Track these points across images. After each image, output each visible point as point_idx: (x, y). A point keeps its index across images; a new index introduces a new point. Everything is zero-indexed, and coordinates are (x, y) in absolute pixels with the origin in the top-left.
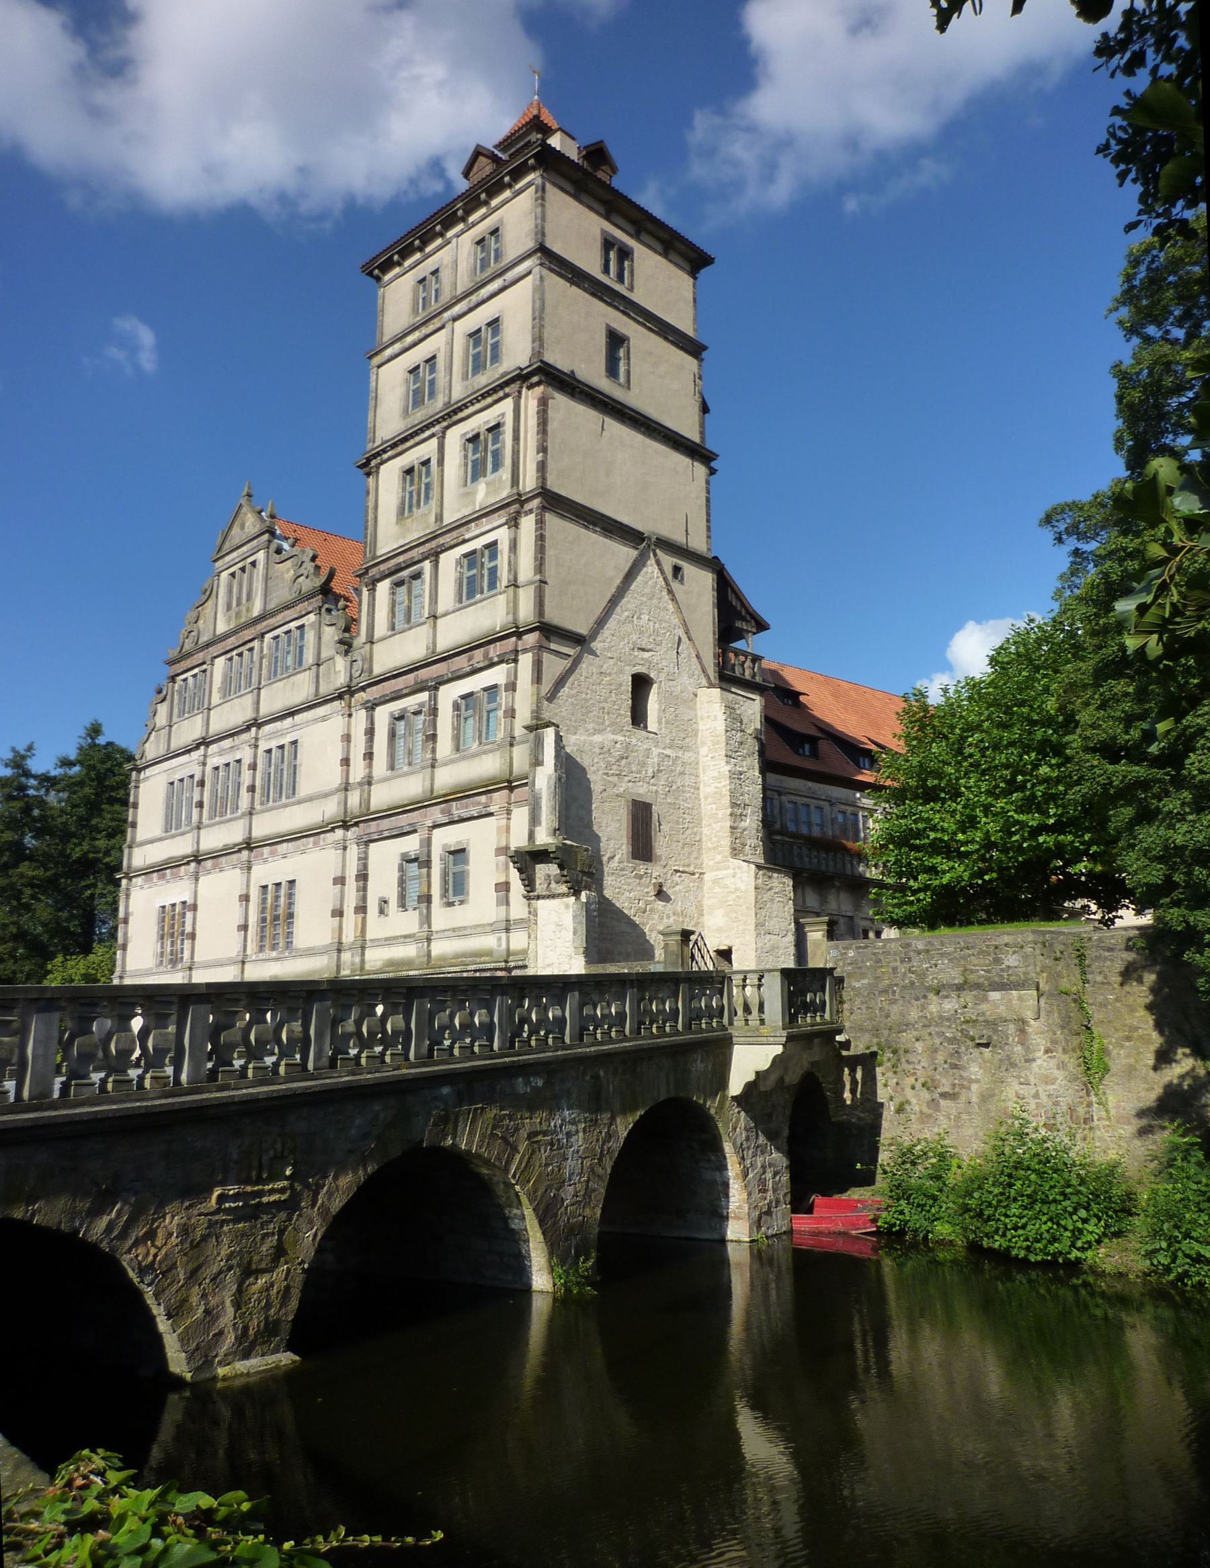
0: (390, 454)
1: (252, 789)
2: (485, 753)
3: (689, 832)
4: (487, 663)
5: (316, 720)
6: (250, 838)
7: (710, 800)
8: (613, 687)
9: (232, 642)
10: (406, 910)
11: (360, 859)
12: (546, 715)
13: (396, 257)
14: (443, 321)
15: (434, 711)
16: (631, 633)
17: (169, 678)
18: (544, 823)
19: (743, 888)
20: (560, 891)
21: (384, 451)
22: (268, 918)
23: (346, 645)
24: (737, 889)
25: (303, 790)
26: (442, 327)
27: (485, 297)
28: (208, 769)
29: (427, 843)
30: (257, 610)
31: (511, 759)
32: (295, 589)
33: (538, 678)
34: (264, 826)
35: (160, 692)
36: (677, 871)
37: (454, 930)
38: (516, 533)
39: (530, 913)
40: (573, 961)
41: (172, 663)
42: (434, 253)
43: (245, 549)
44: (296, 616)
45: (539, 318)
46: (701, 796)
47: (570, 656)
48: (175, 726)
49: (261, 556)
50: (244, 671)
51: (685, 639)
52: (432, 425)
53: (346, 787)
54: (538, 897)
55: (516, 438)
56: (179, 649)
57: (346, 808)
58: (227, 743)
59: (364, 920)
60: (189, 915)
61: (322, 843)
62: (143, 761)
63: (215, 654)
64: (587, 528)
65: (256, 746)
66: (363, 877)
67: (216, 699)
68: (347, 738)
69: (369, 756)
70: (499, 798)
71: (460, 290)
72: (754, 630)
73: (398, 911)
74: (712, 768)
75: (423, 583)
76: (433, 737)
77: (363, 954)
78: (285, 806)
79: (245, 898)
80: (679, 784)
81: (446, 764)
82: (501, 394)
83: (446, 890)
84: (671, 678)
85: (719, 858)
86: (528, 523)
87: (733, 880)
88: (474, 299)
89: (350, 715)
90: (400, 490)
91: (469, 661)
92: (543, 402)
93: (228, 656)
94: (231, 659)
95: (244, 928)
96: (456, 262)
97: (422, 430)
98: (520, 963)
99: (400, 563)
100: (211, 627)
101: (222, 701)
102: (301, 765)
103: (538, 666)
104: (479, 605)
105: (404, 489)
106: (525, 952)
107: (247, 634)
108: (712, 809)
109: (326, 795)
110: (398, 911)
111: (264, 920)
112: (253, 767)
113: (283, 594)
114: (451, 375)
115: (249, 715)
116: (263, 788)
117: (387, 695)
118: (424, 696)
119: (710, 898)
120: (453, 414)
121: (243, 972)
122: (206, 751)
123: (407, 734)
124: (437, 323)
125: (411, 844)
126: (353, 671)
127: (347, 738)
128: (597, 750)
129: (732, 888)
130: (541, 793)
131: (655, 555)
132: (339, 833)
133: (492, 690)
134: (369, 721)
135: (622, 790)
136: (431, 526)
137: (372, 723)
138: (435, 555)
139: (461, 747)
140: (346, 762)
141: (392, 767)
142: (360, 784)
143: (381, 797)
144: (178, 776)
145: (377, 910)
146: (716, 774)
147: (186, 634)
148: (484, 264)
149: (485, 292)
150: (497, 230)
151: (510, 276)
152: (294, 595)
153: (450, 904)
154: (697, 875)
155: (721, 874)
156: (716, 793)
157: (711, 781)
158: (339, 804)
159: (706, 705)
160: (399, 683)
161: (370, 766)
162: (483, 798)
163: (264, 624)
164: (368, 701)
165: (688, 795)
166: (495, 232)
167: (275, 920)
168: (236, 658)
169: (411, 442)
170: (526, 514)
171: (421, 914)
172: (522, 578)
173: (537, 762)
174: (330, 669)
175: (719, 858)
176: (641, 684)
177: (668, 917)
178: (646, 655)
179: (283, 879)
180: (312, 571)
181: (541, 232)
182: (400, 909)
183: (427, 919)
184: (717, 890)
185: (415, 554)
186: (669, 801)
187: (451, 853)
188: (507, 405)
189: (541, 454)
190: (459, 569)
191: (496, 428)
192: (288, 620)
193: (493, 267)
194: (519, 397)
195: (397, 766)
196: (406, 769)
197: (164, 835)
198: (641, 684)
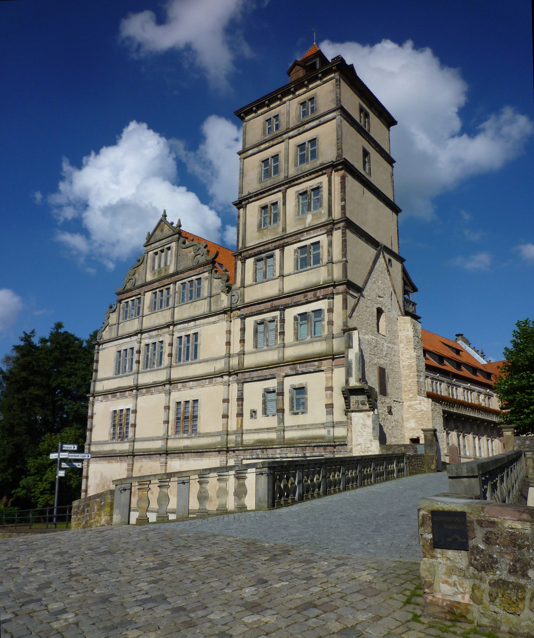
0: (254, 199)
1: (170, 355)
2: (316, 341)
3: (397, 383)
4: (316, 298)
5: (209, 323)
6: (170, 379)
7: (406, 368)
8: (371, 313)
9: (156, 285)
10: (268, 416)
11: (238, 391)
12: (351, 325)
13: (254, 108)
14: (283, 139)
15: (283, 321)
16: (376, 289)
17: (118, 301)
18: (354, 376)
19: (425, 409)
20: (365, 409)
21: (251, 198)
22: (182, 418)
23: (229, 289)
24: (422, 410)
25: (202, 355)
26: (283, 141)
27: (308, 128)
28: (143, 345)
29: (281, 384)
30: (172, 270)
31: (333, 344)
32: (195, 261)
33: (345, 307)
34: (177, 373)
35: (111, 307)
36: (394, 401)
37: (298, 426)
38: (331, 238)
39: (348, 419)
40: (373, 443)
41: (119, 294)
42: (276, 108)
43: (164, 241)
44: (196, 273)
45: (340, 139)
46: (401, 366)
47: (356, 297)
48: (122, 324)
49: (174, 245)
50: (164, 299)
51: (393, 293)
52: (280, 186)
53: (229, 356)
54: (353, 411)
55: (330, 193)
56: (123, 287)
57: (229, 366)
58: (154, 333)
59: (242, 420)
60: (132, 416)
61: (214, 382)
62: (102, 340)
63: (146, 290)
64: (360, 238)
65: (173, 335)
66: (240, 399)
67: (146, 311)
68: (229, 332)
69: (242, 341)
70: (325, 365)
71: (291, 126)
72: (412, 291)
73: (262, 416)
74: (406, 353)
75: (274, 260)
76: (283, 333)
77: (242, 437)
78: (191, 364)
79: (167, 408)
80: (394, 360)
81: (291, 346)
82: (321, 173)
83: (293, 407)
84: (389, 311)
85: (411, 395)
86: (337, 235)
87: (419, 406)
88: (301, 129)
89: (231, 321)
90: (259, 216)
91: (304, 297)
92: (343, 178)
93: (154, 291)
94: (155, 293)
95: (167, 422)
96: (288, 113)
97: (274, 188)
98: (343, 443)
99: (261, 250)
100: (144, 278)
101: (150, 313)
102: (200, 345)
103: (345, 301)
104: (309, 271)
105: (261, 216)
106: (345, 438)
107: (166, 281)
108: (407, 372)
109: (216, 359)
110: (262, 416)
111: (178, 419)
112: (171, 345)
113: (188, 263)
114: (288, 163)
115: (169, 319)
116: (176, 355)
117: (254, 312)
118: (277, 313)
119: (407, 414)
120: (291, 182)
121: (167, 444)
122: (141, 337)
123: (266, 331)
124: (279, 139)
125: (272, 384)
126: (232, 300)
127: (229, 332)
128: (367, 342)
129: (419, 410)
130: (352, 362)
131: (383, 253)
132: (226, 378)
133: (318, 312)
134: (242, 325)
135: (376, 361)
136: (279, 232)
137: (244, 325)
138: (282, 248)
139: (299, 338)
140: (228, 343)
141: (256, 346)
142: (238, 354)
143: (250, 361)
144: (123, 348)
145: (249, 415)
146: (409, 356)
147: (128, 280)
148: (305, 114)
150: (313, 98)
151: (323, 119)
152: (195, 264)
153: (297, 414)
154: (401, 403)
155: (413, 403)
156: (409, 365)
157: (406, 360)
158: (225, 363)
159: (403, 324)
160: (262, 307)
161: (243, 346)
162: (316, 363)
163: (177, 277)
164: (242, 315)
165: (397, 366)
166: (312, 99)
167: (185, 419)
168: (158, 293)
169: (267, 194)
170: (336, 229)
171: (279, 418)
172: (335, 259)
173: (349, 346)
174: (218, 299)
175: (411, 395)
176: (380, 312)
177: (393, 423)
178: (381, 299)
179: (190, 399)
180: (206, 252)
181: (338, 100)
182: (264, 415)
183: (281, 421)
184: (411, 410)
185: (270, 246)
186: (391, 368)
187: (295, 389)
188: (324, 179)
189: (344, 202)
190: (296, 254)
191: (317, 189)
192: (191, 275)
193: (310, 116)
194: (331, 175)
195: (259, 346)
196: (265, 348)
197: (115, 376)
198: (380, 312)
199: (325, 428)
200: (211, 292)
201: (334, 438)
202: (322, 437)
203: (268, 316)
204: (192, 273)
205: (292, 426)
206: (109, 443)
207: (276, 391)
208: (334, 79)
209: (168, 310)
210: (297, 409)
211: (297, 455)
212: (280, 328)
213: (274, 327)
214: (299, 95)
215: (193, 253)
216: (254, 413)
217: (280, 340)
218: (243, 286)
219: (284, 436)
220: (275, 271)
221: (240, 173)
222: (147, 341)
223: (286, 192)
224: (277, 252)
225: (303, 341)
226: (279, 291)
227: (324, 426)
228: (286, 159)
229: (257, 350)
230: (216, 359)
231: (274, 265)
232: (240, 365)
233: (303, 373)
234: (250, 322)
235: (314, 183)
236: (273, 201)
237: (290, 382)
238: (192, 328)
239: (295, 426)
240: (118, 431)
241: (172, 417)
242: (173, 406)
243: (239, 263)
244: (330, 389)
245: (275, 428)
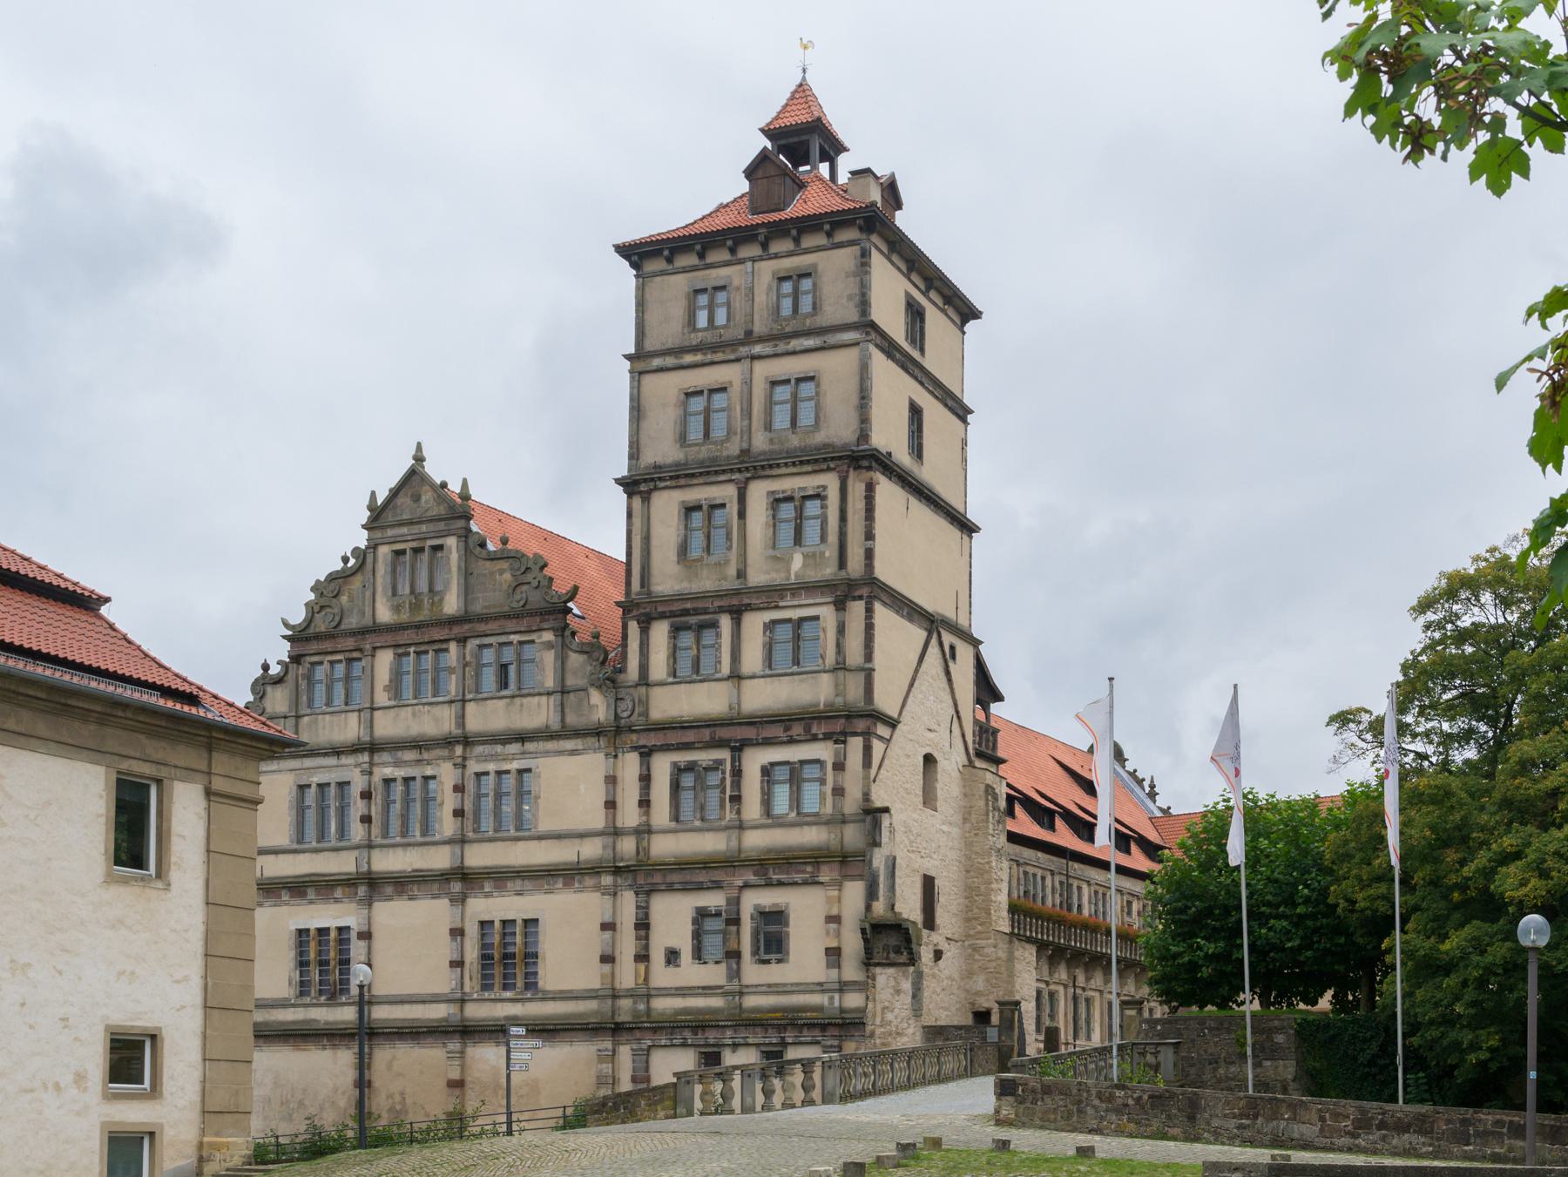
0: (668, 483)
4: (808, 737)
5: (560, 753)
10: (705, 963)
11: (638, 907)
15: (737, 773)
18: (881, 899)
26: (738, 360)
39: (868, 977)
55: (843, 518)
66: (643, 926)
68: (611, 780)
69: (645, 803)
75: (718, 635)
76: (737, 799)
79: (457, 933)
83: (759, 949)
89: (616, 756)
101: (392, 703)
106: (863, 1010)
107: (437, 634)
109: (583, 835)
123: (699, 788)
125: (714, 900)
134: (644, 767)
138: (737, 613)
141: (676, 817)
143: (665, 847)
144: (316, 779)
153: (768, 962)
160: (690, 736)
170: (854, 599)
171: (729, 968)
183: (735, 974)
187: (761, 913)
190: (768, 633)
196: (698, 823)
197: (295, 846)
199: (823, 991)
200: (563, 679)
201: (842, 1010)
202: (819, 1008)
203: (704, 757)
204: (510, 625)
205: (756, 986)
206: (294, 1006)
207: (724, 914)
208: (858, 247)
209: (446, 706)
210: (766, 953)
211: (767, 1040)
212: (732, 786)
213: (719, 782)
214: (776, 256)
215: (507, 576)
216: (672, 956)
217: (731, 812)
218: (644, 680)
219: (741, 1004)
220: (720, 662)
221: (632, 408)
222: (388, 771)
223: (745, 488)
224: (725, 622)
225: (781, 820)
226: (731, 708)
227: (821, 987)
228: (745, 407)
229: (679, 826)
230: (583, 835)
231: (717, 647)
232: (642, 853)
233: (781, 884)
234: (662, 766)
235: (810, 483)
236: (715, 498)
237: (754, 900)
238: (513, 758)
239: (762, 985)
240: (317, 978)
241: (472, 954)
242: (472, 931)
243: (633, 627)
244: (834, 919)
245: (721, 987)
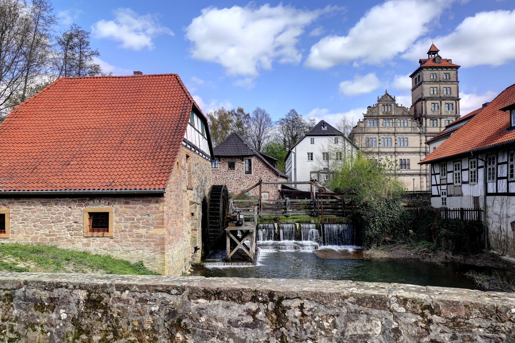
68: (421, 140)
88: (446, 83)
138: (440, 119)
149: (448, 83)
218: (426, 127)
235: (451, 102)
238: (405, 136)
242: (399, 160)
